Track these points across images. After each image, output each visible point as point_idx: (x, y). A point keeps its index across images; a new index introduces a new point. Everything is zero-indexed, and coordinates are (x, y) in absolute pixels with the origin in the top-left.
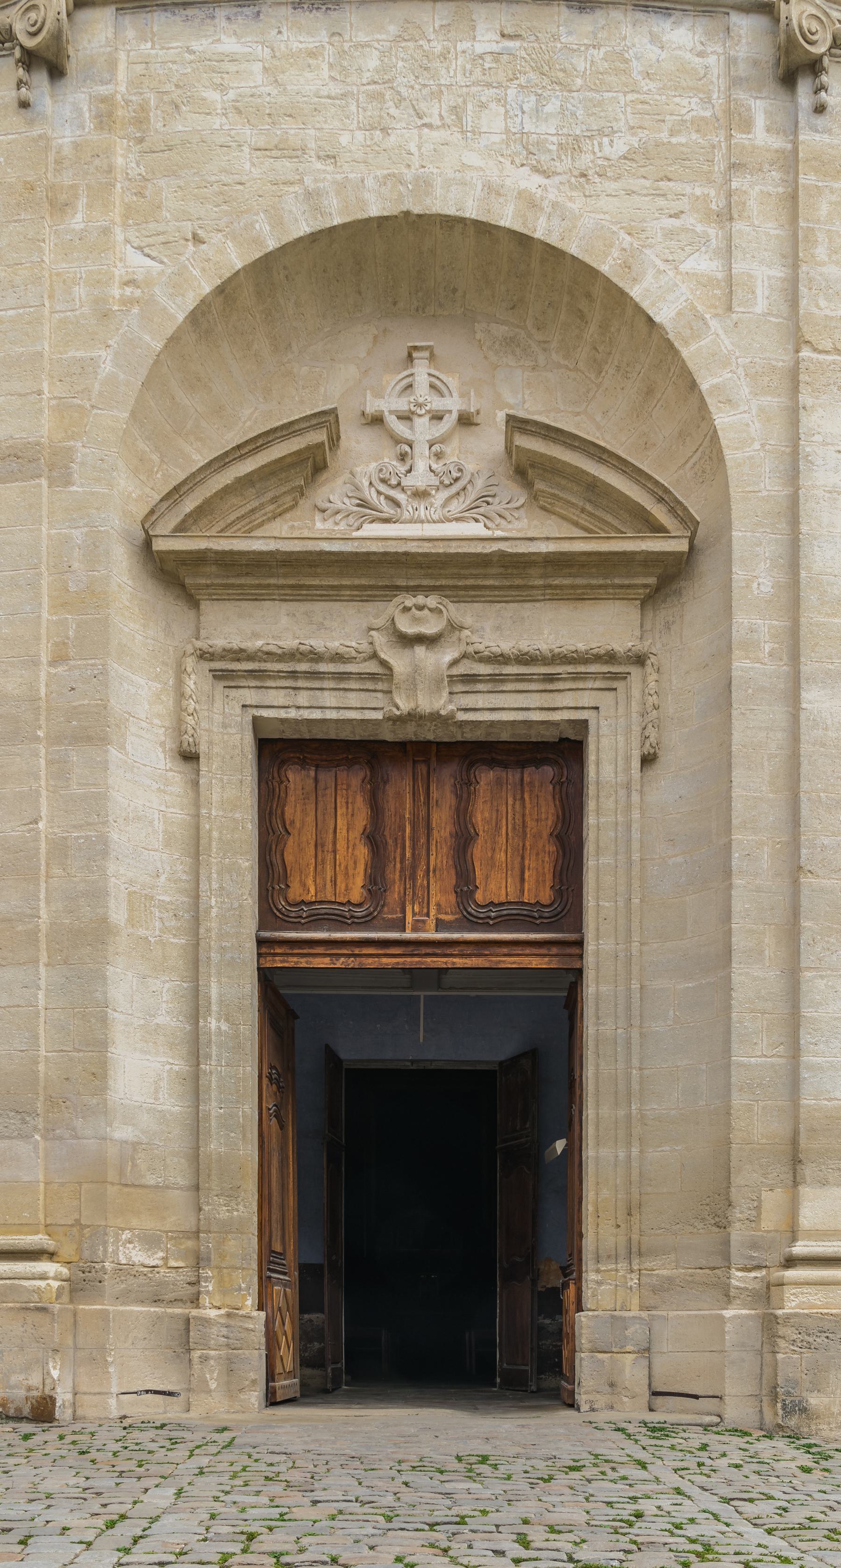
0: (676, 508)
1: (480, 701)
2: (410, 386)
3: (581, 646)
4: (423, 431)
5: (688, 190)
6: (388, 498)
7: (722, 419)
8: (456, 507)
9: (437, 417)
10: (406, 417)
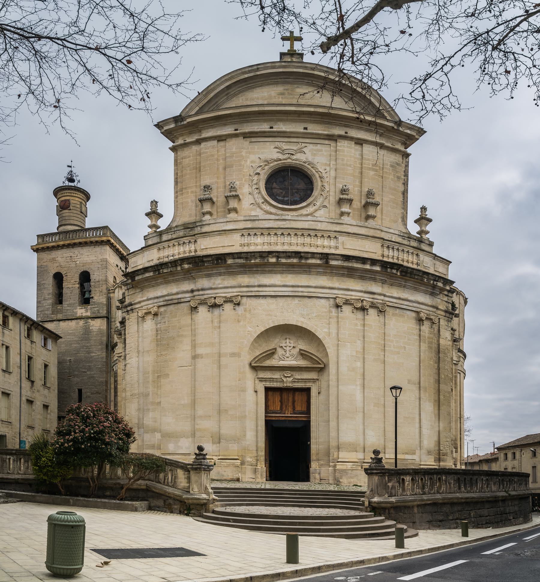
0: (322, 361)
4: (288, 349)
7: (328, 350)
8: (293, 359)
10: (286, 347)
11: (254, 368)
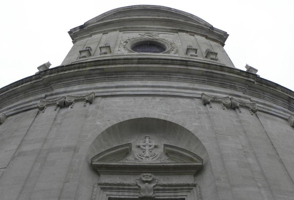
1: (161, 194)
2: (145, 142)
3: (182, 183)
4: (147, 148)
5: (192, 116)
6: (140, 158)
9: (150, 146)
10: (144, 146)
11: (96, 170)
